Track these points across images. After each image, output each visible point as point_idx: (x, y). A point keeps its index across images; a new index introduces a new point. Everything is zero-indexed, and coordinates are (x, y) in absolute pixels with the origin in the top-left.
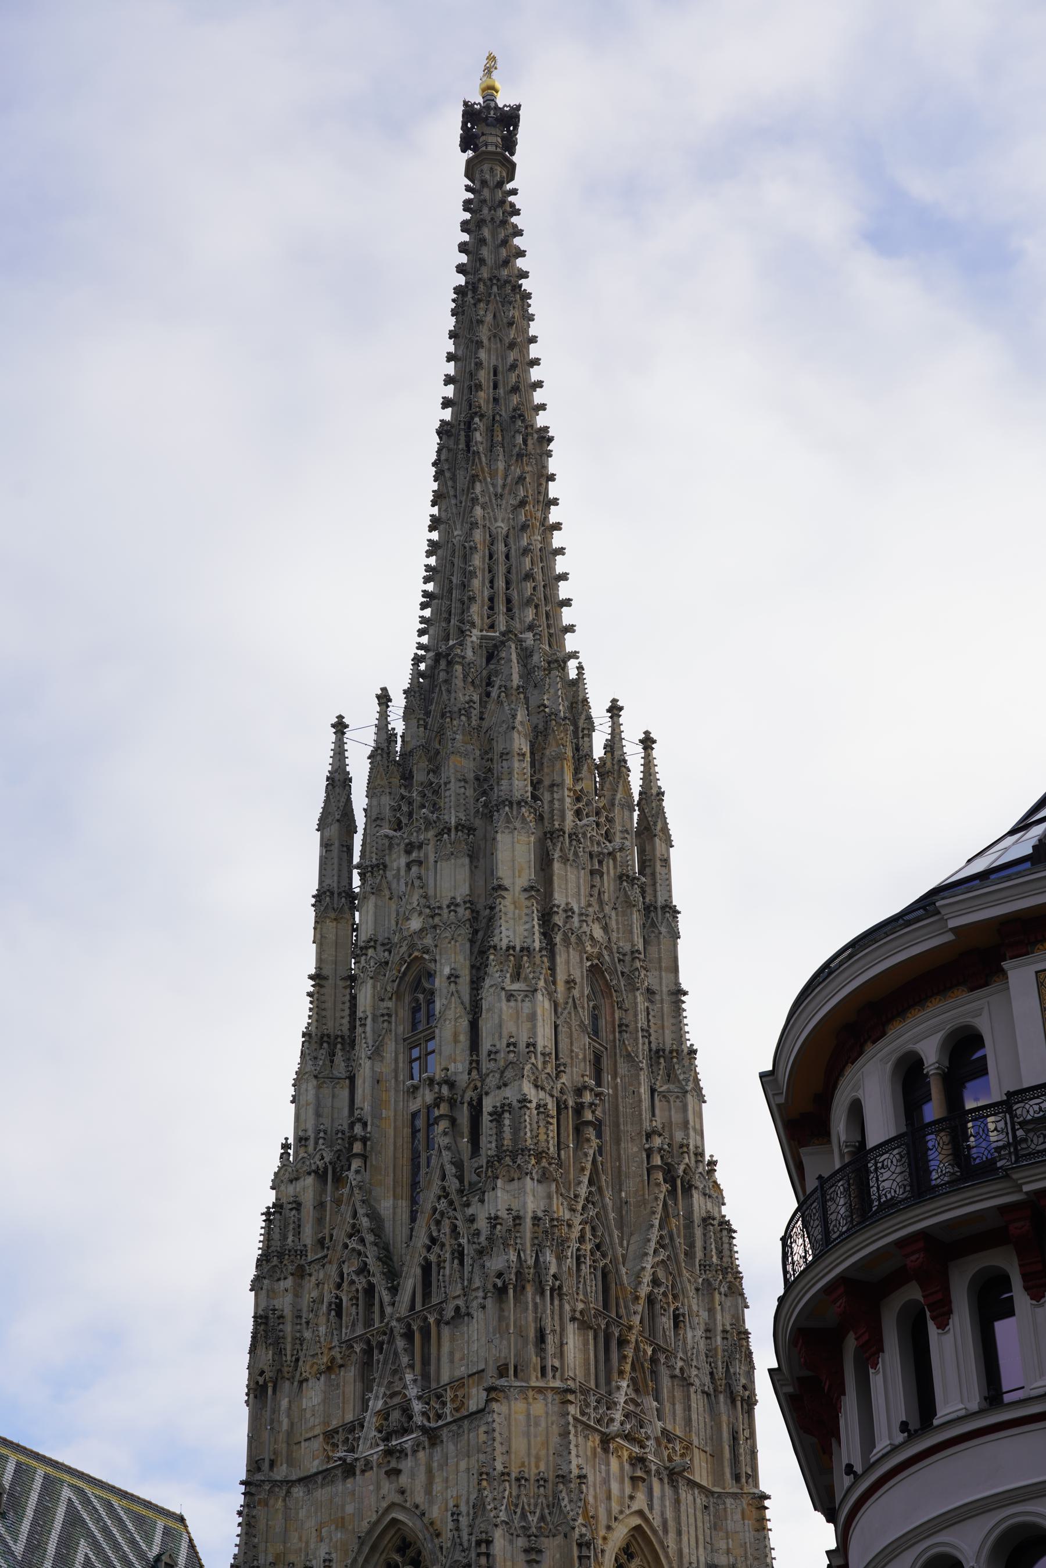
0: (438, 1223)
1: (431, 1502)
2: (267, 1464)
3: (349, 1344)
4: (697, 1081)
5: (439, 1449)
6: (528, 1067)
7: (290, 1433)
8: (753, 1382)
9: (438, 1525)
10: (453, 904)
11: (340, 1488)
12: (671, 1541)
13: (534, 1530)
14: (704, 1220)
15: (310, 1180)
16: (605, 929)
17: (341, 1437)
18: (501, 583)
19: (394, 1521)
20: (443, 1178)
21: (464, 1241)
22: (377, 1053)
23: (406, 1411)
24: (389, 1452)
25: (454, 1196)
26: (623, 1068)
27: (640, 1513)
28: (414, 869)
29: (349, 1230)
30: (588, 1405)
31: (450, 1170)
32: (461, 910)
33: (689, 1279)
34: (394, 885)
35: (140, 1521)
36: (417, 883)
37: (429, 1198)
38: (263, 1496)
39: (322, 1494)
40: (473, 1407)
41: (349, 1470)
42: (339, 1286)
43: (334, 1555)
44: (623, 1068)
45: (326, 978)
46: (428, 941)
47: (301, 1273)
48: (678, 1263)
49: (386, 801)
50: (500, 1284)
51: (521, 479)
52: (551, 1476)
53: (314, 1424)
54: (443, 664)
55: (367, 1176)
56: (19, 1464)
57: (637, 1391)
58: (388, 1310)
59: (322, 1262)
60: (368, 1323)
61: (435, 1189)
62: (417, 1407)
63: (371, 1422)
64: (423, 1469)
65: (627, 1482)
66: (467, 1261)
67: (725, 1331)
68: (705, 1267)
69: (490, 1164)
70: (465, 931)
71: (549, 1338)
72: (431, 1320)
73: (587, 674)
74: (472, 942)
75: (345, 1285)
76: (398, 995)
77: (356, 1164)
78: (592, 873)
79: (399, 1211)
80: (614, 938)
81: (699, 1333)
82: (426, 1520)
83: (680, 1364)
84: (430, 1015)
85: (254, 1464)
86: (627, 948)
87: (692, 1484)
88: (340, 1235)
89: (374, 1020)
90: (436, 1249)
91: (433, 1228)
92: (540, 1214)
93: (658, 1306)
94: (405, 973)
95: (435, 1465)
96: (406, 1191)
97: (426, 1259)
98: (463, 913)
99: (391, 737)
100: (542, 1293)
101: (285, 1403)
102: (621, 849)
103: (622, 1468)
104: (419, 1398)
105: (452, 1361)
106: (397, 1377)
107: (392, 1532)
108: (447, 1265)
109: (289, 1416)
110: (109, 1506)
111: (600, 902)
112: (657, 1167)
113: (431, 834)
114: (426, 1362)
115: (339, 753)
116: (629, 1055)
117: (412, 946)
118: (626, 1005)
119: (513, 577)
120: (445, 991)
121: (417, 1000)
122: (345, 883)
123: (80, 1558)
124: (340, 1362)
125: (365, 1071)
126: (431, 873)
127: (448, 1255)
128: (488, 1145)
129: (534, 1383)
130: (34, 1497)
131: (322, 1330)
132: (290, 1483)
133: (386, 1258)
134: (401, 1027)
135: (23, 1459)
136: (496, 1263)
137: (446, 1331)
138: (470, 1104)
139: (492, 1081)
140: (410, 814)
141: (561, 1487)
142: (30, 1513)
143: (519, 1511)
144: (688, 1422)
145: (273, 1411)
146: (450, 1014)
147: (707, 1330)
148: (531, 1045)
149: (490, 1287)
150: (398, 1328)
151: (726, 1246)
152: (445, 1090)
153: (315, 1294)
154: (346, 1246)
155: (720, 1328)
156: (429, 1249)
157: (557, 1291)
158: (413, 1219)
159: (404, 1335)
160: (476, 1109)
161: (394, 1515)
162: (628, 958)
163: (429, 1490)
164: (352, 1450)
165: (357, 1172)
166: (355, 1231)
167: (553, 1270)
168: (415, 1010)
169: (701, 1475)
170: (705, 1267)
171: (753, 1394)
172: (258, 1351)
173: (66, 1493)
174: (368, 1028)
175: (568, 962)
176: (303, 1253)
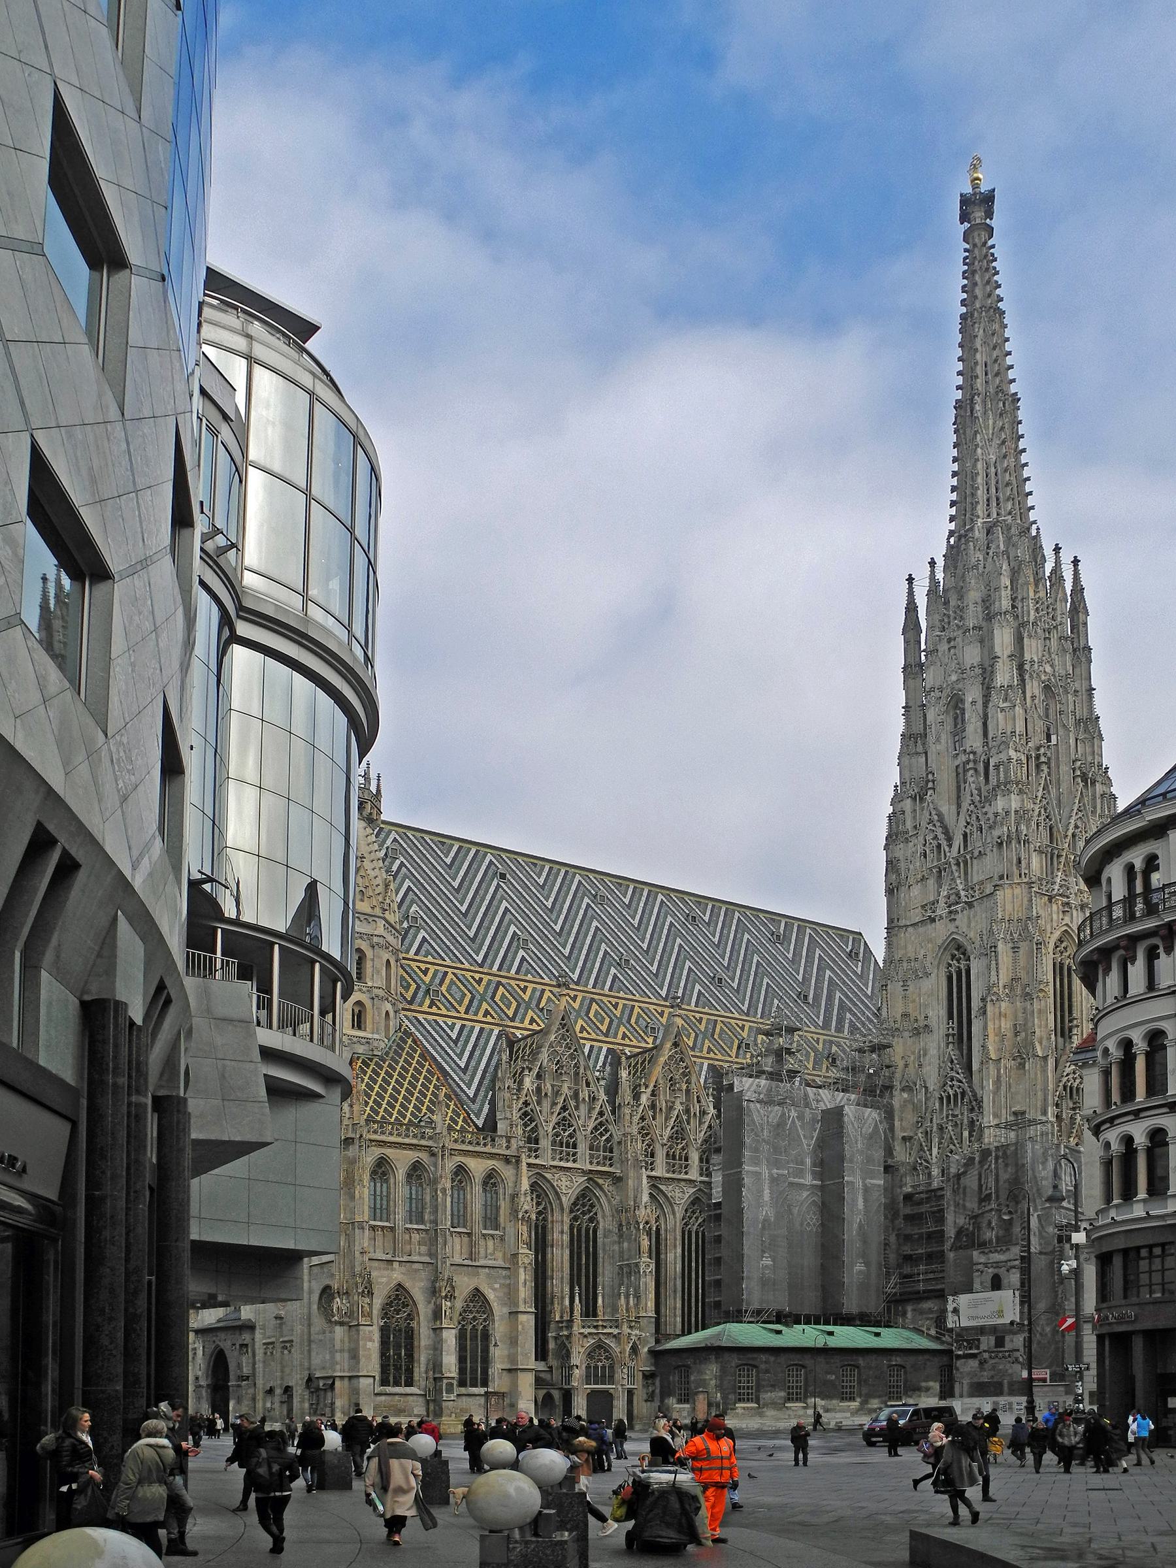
21: (982, 823)
23: (958, 895)
37: (965, 805)
39: (921, 930)
40: (988, 893)
41: (933, 920)
42: (925, 845)
53: (918, 903)
58: (948, 854)
60: (939, 859)
62: (963, 893)
63: (942, 901)
84: (963, 720)
88: (924, 824)
90: (969, 827)
114: (966, 873)
123: (817, 956)
132: (907, 926)
137: (975, 861)
139: (994, 751)
142: (793, 941)
146: (973, 720)
152: (971, 756)
158: (958, 814)
163: (969, 926)
164: (934, 912)
166: (931, 821)
168: (956, 719)
174: (933, 730)
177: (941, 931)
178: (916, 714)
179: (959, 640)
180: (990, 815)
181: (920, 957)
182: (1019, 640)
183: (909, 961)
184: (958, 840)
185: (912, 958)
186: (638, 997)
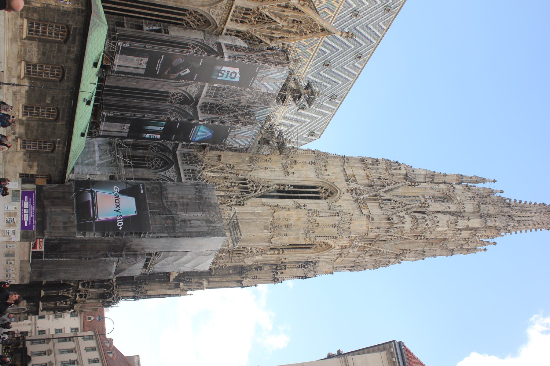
0: (399, 203)
1: (342, 200)
2: (348, 161)
3: (373, 181)
4: (417, 260)
5: (353, 202)
6: (434, 226)
7: (354, 166)
8: (355, 271)
9: (337, 202)
10: (464, 208)
11: (343, 178)
12: (327, 253)
13: (339, 226)
14: (389, 261)
15: (405, 172)
16: (453, 241)
17: (354, 179)
18: (523, 218)
19: (337, 191)
20: (409, 205)
22: (432, 188)
24: (352, 190)
25: (406, 207)
26: (424, 244)
27: (335, 247)
28: (469, 198)
29: (396, 181)
30: (360, 237)
31: (411, 206)
32: (463, 209)
33: (378, 258)
34: (465, 193)
35: (322, 129)
36: (467, 199)
37: (404, 201)
38: (342, 160)
39: (341, 174)
41: (347, 180)
43: (329, 176)
44: (424, 244)
45: (445, 177)
46: (455, 201)
47: (387, 170)
48: (383, 255)
49: (482, 192)
50: (391, 219)
51: (543, 224)
52: (350, 230)
54: (508, 205)
55: (407, 186)
56: (338, 103)
57: (359, 247)
58: (381, 191)
59: (389, 175)
61: (407, 203)
63: (357, 186)
64: (349, 198)
65: (341, 245)
66: (393, 210)
67: (366, 265)
68: (380, 261)
69: (414, 216)
70: (459, 211)
71: (378, 230)
72: (380, 201)
73: (502, 237)
74: (456, 212)
75: (385, 180)
76: (443, 194)
77: (410, 183)
78: (465, 239)
79: (399, 193)
80: (451, 243)
81: (367, 260)
82: (338, 199)
83: (362, 256)
85: (347, 159)
86: (448, 246)
87: (337, 258)
89: (439, 188)
90: (394, 202)
91: (399, 202)
92: (404, 228)
93: (375, 251)
94: (447, 195)
95: (350, 201)
96: (403, 195)
97: (392, 200)
98: (462, 210)
99: (494, 193)
100: (387, 229)
101: (360, 165)
102: (468, 245)
103: (345, 244)
104: (364, 198)
105: (371, 206)
106: (367, 192)
107: (335, 191)
108: (391, 205)
109: (357, 166)
110: (325, 123)
111: (459, 240)
112: (403, 252)
113: (476, 203)
114: (370, 199)
115: (489, 181)
116: (426, 246)
117: (454, 198)
118: (437, 245)
119: (525, 221)
120: (446, 205)
121: (442, 198)
122: (464, 181)
124: (369, 178)
125: (428, 186)
126: (469, 202)
127: (393, 205)
128: (417, 215)
129: (370, 226)
130: (331, 107)
131: (375, 175)
133: (391, 190)
134: (437, 194)
135: (339, 104)
136: (395, 218)
138: (425, 211)
139: (430, 217)
140: (480, 197)
141: (348, 232)
143: (344, 222)
144: (350, 257)
145: (358, 163)
147: (367, 261)
148: (438, 226)
149: (390, 216)
150: (377, 193)
151: (383, 266)
153: (382, 173)
154: (393, 181)
155: (367, 264)
156: (394, 201)
157: (388, 232)
159: (376, 194)
160: (424, 213)
161: (339, 191)
162: (446, 246)
165: (408, 184)
167: (392, 231)
169: (340, 259)
170: (380, 261)
171: (353, 271)
172: (371, 160)
173: (331, 113)
175: (450, 234)
176: (390, 170)
177: (341, 185)
178: (441, 179)
179: (473, 202)
180: (402, 214)
181: (327, 172)
182: (471, 229)
183: (325, 166)
184: (387, 196)
185: (326, 168)
186: (337, 16)
